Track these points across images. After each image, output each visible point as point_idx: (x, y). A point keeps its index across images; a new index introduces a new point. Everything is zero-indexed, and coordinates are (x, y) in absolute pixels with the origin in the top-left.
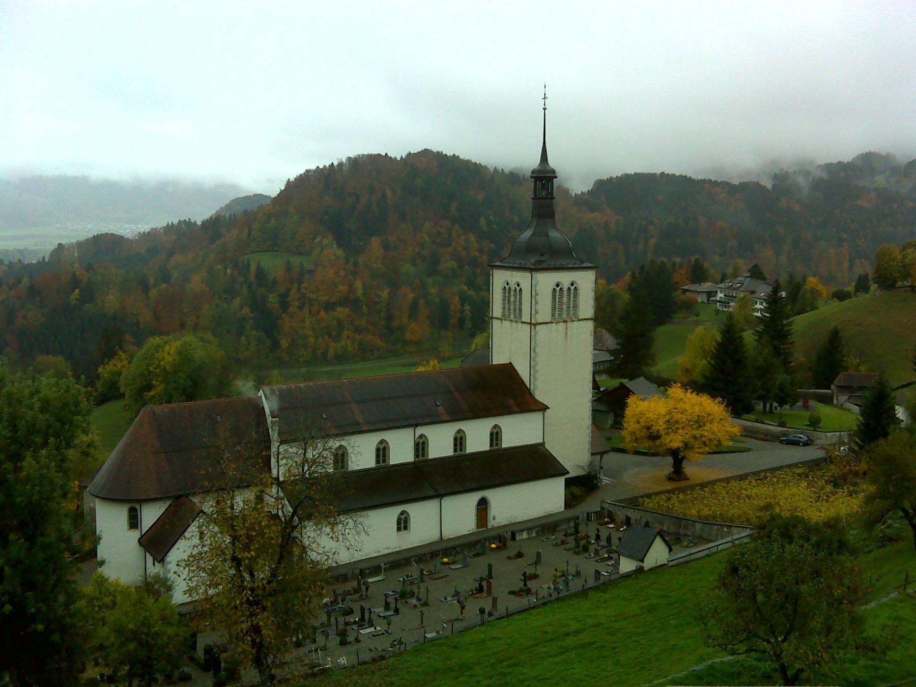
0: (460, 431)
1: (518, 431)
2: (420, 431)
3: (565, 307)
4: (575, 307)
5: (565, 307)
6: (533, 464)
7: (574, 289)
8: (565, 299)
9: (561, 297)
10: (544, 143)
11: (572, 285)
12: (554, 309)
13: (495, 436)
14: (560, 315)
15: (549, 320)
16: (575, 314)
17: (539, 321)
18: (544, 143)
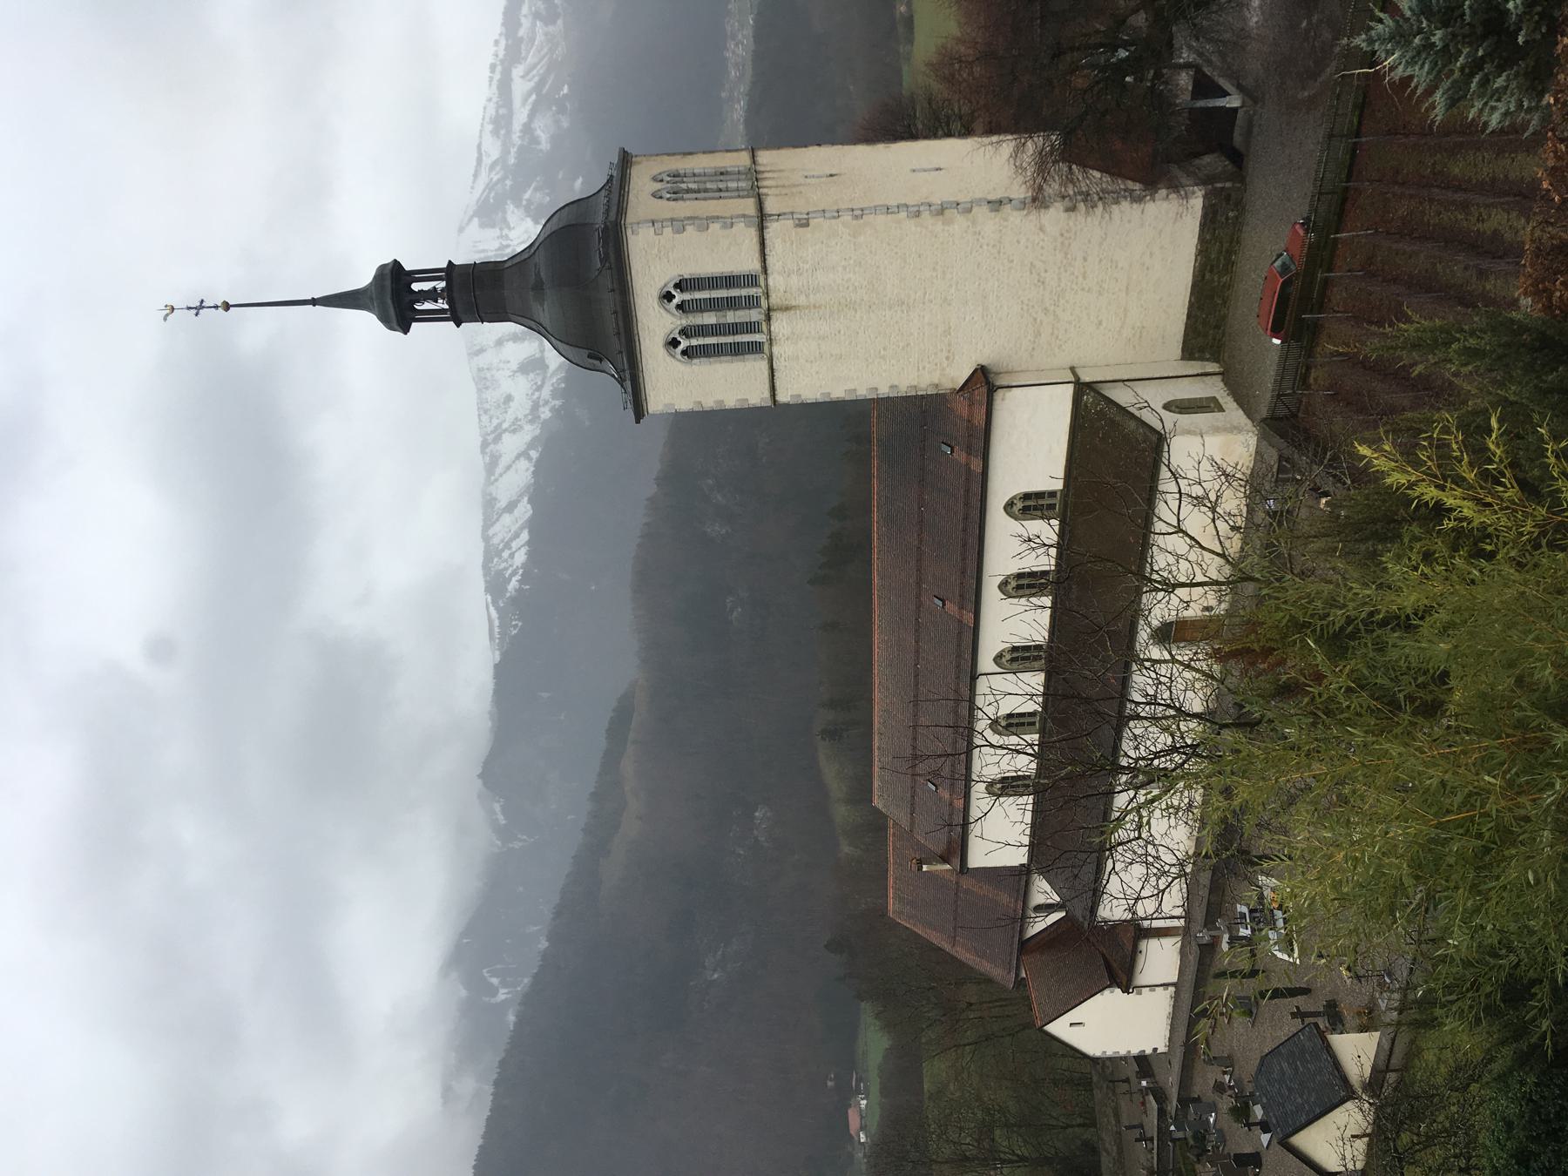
0: (1003, 586)
1: (1031, 447)
2: (986, 663)
3: (731, 317)
4: (730, 281)
5: (731, 317)
6: (1113, 460)
7: (686, 292)
8: (710, 319)
9: (702, 331)
10: (314, 302)
11: (668, 297)
12: (737, 350)
13: (1029, 505)
14: (751, 327)
15: (764, 365)
16: (751, 280)
17: (767, 394)
18: (314, 302)
